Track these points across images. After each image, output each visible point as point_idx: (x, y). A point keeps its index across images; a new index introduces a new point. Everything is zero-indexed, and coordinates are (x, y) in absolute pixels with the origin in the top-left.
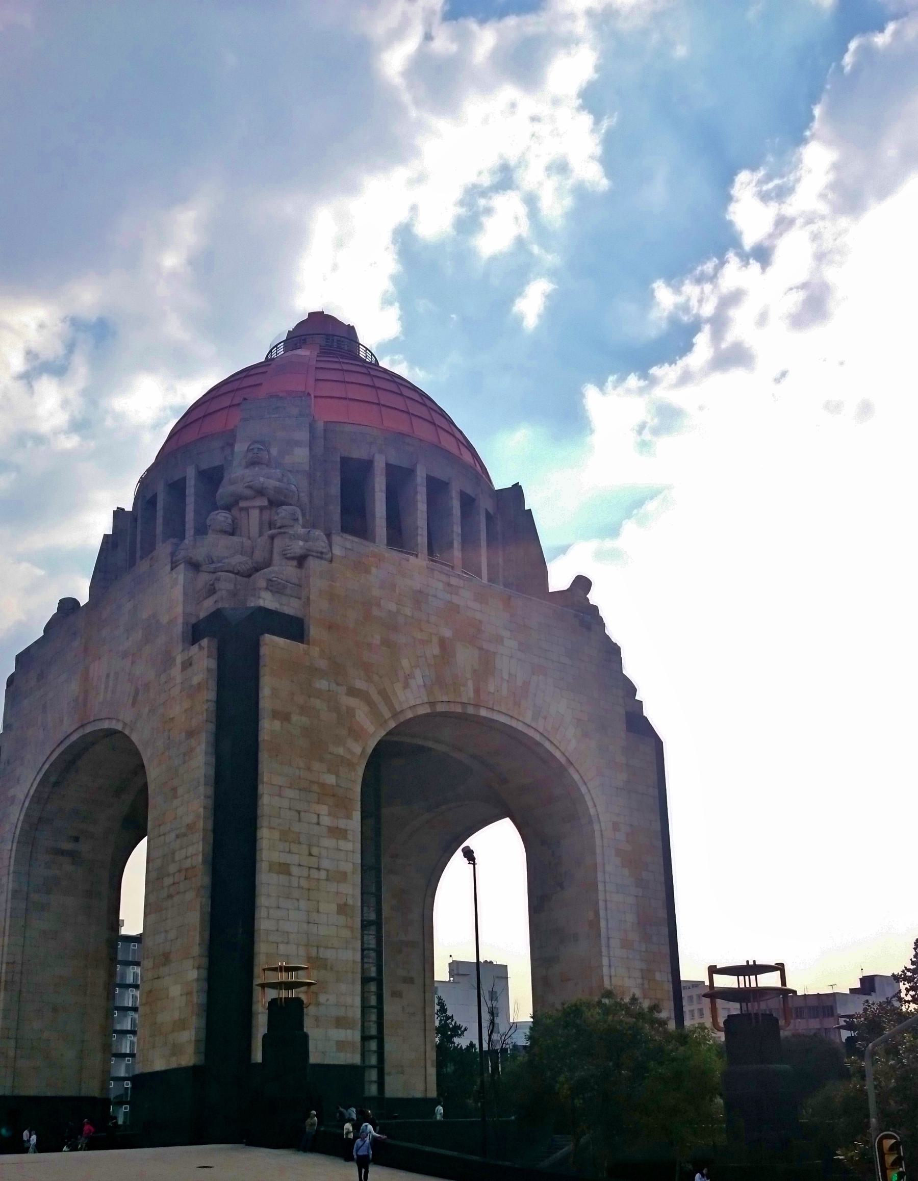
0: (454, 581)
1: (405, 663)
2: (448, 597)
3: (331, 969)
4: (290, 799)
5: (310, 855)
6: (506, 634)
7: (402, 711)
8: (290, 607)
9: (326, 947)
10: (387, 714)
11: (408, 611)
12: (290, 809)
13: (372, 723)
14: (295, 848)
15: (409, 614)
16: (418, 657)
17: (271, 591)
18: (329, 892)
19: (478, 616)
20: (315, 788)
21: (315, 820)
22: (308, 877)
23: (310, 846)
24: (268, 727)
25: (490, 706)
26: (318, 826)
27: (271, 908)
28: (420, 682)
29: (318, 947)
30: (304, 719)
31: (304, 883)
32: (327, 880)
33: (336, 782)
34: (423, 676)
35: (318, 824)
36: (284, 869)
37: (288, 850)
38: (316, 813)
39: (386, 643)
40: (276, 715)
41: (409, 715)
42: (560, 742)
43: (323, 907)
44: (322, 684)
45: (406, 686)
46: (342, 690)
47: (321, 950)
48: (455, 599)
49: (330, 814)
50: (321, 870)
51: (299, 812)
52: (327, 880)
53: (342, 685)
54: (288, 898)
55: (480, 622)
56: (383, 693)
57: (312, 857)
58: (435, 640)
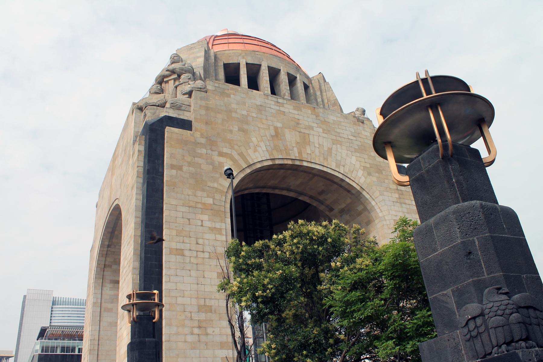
1: (254, 139)
2: (278, 108)
3: (215, 311)
5: (197, 243)
9: (211, 299)
11: (254, 115)
12: (183, 217)
14: (187, 240)
15: (255, 116)
16: (262, 136)
17: (173, 109)
18: (211, 265)
19: (297, 117)
20: (199, 206)
21: (200, 224)
22: (197, 257)
23: (197, 238)
24: (168, 174)
26: (202, 227)
27: (172, 275)
28: (264, 149)
29: (205, 299)
30: (192, 169)
31: (193, 260)
32: (209, 258)
33: (213, 202)
34: (265, 146)
35: (202, 226)
36: (180, 252)
37: (182, 241)
39: (241, 130)
40: (172, 167)
41: (259, 166)
42: (355, 179)
43: (207, 274)
44: (204, 151)
45: (255, 151)
47: (207, 301)
48: (282, 109)
49: (209, 221)
50: (205, 253)
51: (189, 220)
52: (209, 258)
54: (183, 269)
55: (299, 120)
56: (241, 155)
58: (272, 128)
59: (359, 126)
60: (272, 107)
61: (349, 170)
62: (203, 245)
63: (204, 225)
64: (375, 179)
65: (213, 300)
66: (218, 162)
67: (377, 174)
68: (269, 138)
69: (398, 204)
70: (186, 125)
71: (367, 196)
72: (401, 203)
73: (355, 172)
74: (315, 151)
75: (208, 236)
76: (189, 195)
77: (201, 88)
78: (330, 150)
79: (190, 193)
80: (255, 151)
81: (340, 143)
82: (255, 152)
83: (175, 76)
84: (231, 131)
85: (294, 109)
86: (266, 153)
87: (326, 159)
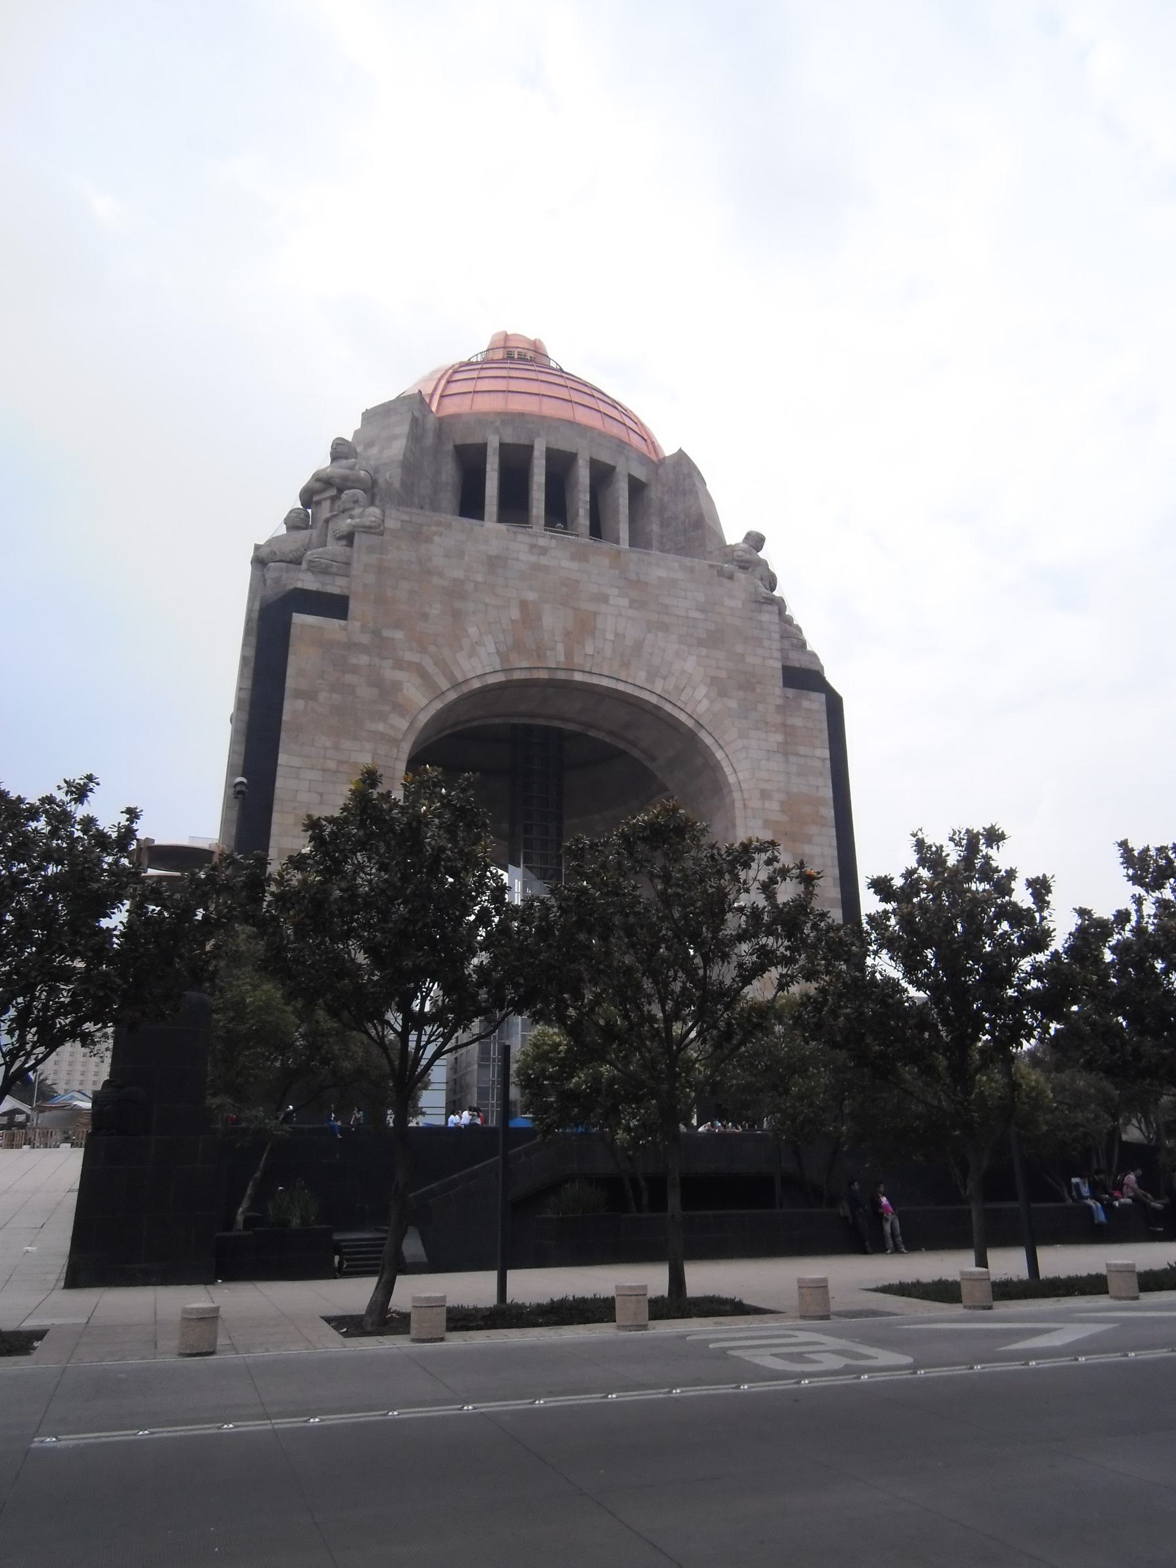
0: (542, 542)
1: (473, 630)
2: (533, 558)
4: (310, 780)
6: (615, 591)
7: (466, 681)
8: (335, 586)
10: (444, 685)
12: (309, 791)
13: (424, 696)
17: (313, 573)
24: (291, 707)
25: (587, 669)
28: (492, 649)
30: (336, 697)
38: (342, 795)
40: (299, 694)
41: (476, 684)
42: (686, 704)
44: (363, 660)
45: (472, 654)
46: (388, 663)
48: (544, 561)
51: (321, 794)
53: (387, 658)
55: (577, 581)
60: (523, 557)
61: (676, 686)
64: (733, 704)
67: (741, 694)
70: (336, 606)
71: (708, 741)
72: (786, 754)
73: (689, 690)
74: (603, 649)
77: (370, 527)
78: (639, 645)
79: (328, 744)
80: (472, 654)
81: (665, 627)
82: (470, 657)
83: (332, 492)
84: (425, 616)
85: (573, 558)
87: (625, 665)
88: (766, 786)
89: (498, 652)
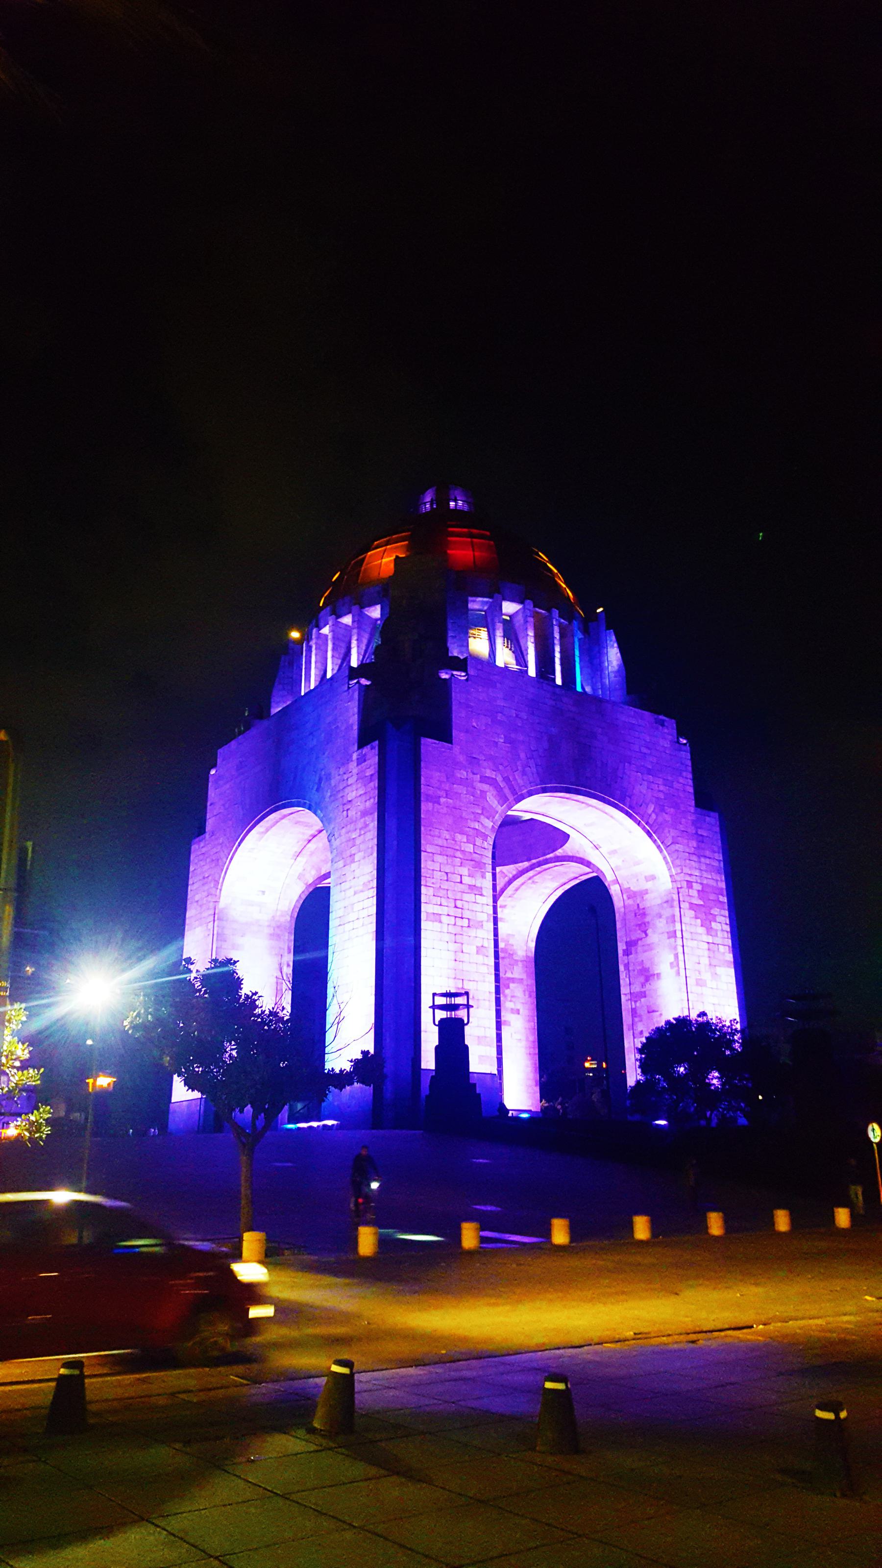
5: (456, 907)
21: (459, 880)
29: (463, 980)
51: (447, 873)
57: (456, 909)
59: (657, 729)
62: (462, 909)
63: (463, 882)
65: (471, 983)
66: (481, 791)
67: (672, 810)
68: (540, 754)
69: (694, 858)
72: (699, 857)
75: (466, 897)
76: (447, 840)
86: (535, 775)
88: (688, 878)
89: (538, 773)
